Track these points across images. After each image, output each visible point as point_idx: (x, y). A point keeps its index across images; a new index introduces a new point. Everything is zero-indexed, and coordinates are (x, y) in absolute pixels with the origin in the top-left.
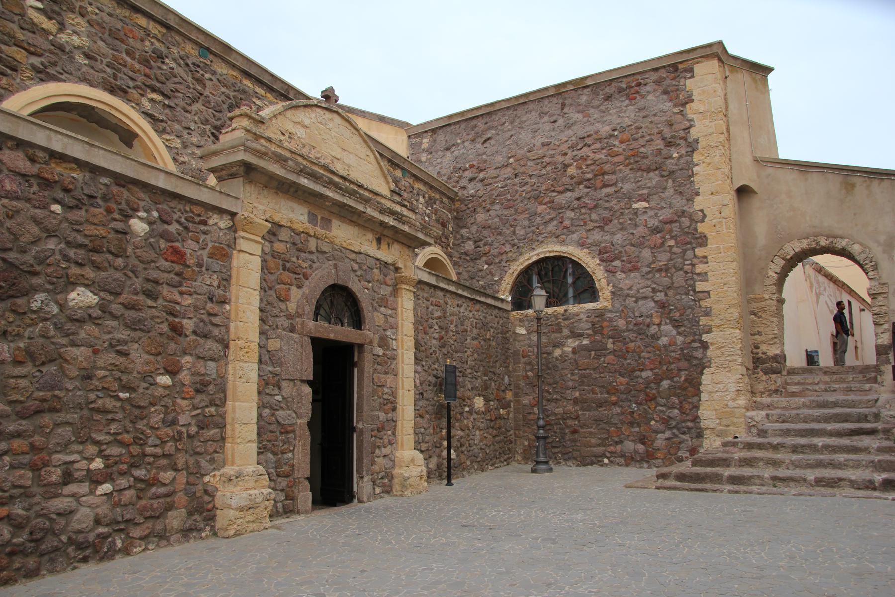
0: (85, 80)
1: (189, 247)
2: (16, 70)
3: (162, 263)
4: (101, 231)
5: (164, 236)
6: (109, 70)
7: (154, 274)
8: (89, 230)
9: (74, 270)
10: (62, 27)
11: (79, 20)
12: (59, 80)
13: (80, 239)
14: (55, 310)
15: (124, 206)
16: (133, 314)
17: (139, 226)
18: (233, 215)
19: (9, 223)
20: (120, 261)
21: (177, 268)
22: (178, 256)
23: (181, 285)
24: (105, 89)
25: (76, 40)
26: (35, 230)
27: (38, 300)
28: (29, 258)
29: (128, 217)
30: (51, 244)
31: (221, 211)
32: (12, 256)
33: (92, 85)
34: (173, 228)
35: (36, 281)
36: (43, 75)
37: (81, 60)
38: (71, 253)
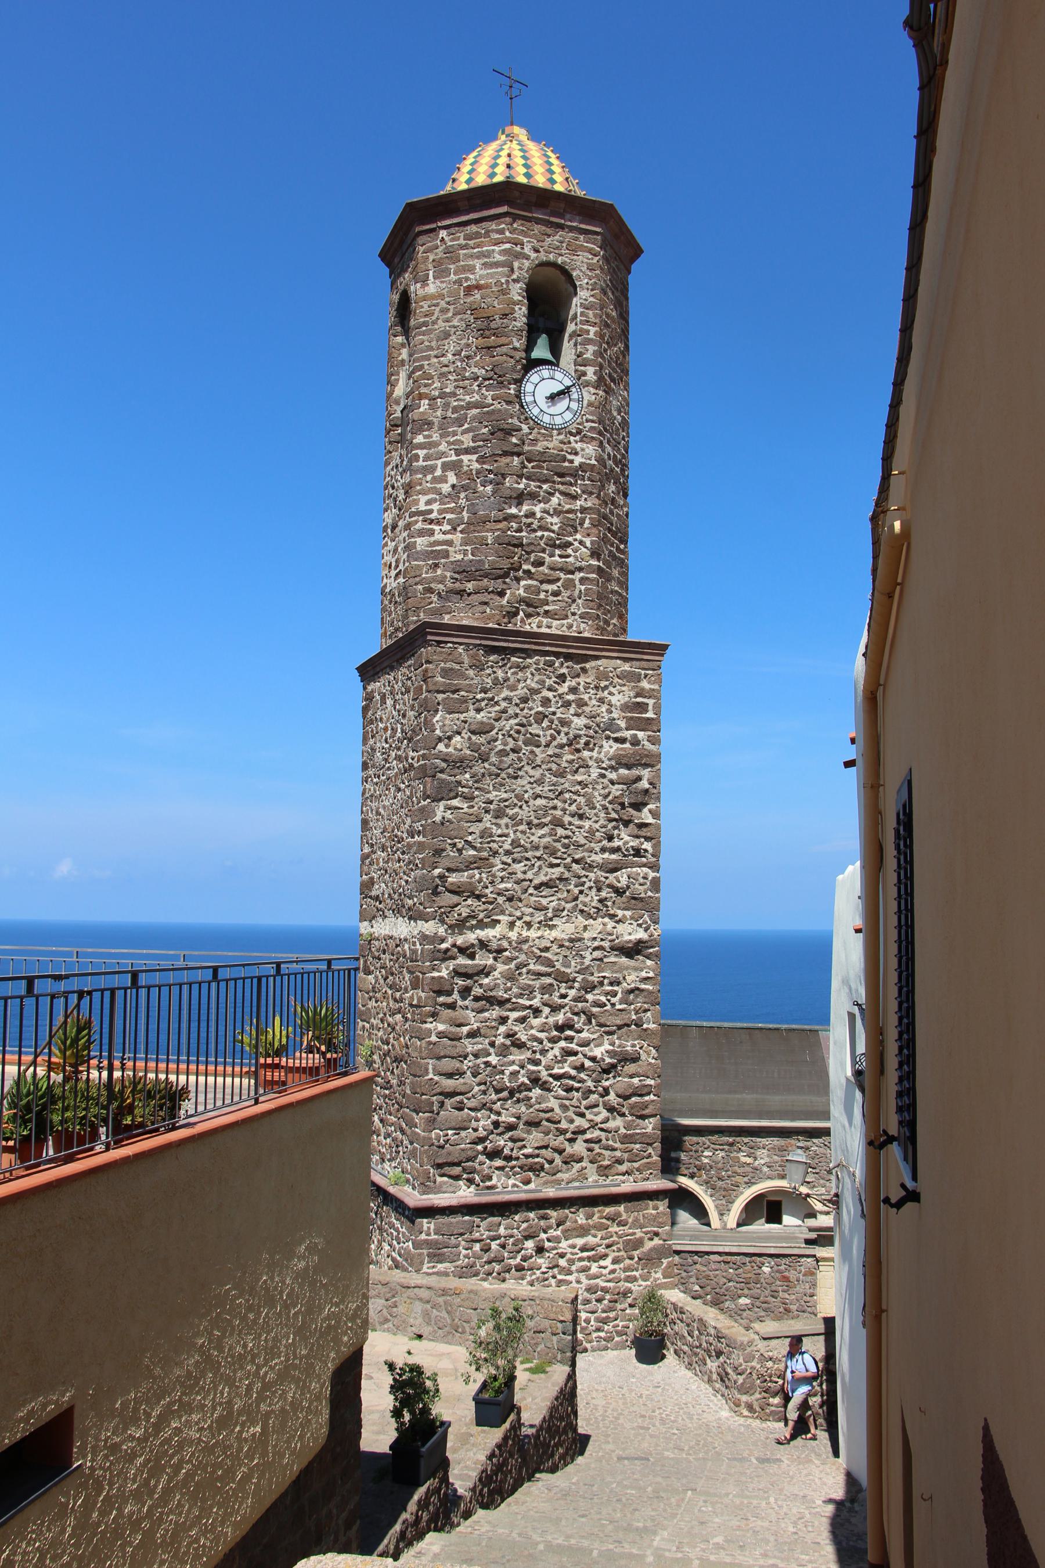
0: (770, 1178)
1: (792, 1275)
2: (738, 1186)
3: (778, 1283)
4: (749, 1275)
5: (778, 1271)
6: (780, 1168)
7: (774, 1288)
8: (744, 1275)
9: (740, 1292)
10: (755, 1159)
11: (763, 1151)
12: (755, 1183)
13: (741, 1280)
14: (734, 1307)
15: (758, 1263)
16: (766, 1305)
17: (766, 1269)
18: (814, 1256)
19: (715, 1280)
20: (758, 1286)
21: (786, 1284)
22: (786, 1279)
23: (788, 1290)
24: (779, 1178)
25: (762, 1162)
26: (725, 1280)
27: (727, 1304)
28: (723, 1290)
29: (761, 1268)
30: (731, 1284)
31: (808, 1256)
32: (716, 1291)
33: (771, 1179)
34: (783, 1267)
35: (727, 1297)
36: (750, 1184)
37: (765, 1169)
38: (738, 1285)
